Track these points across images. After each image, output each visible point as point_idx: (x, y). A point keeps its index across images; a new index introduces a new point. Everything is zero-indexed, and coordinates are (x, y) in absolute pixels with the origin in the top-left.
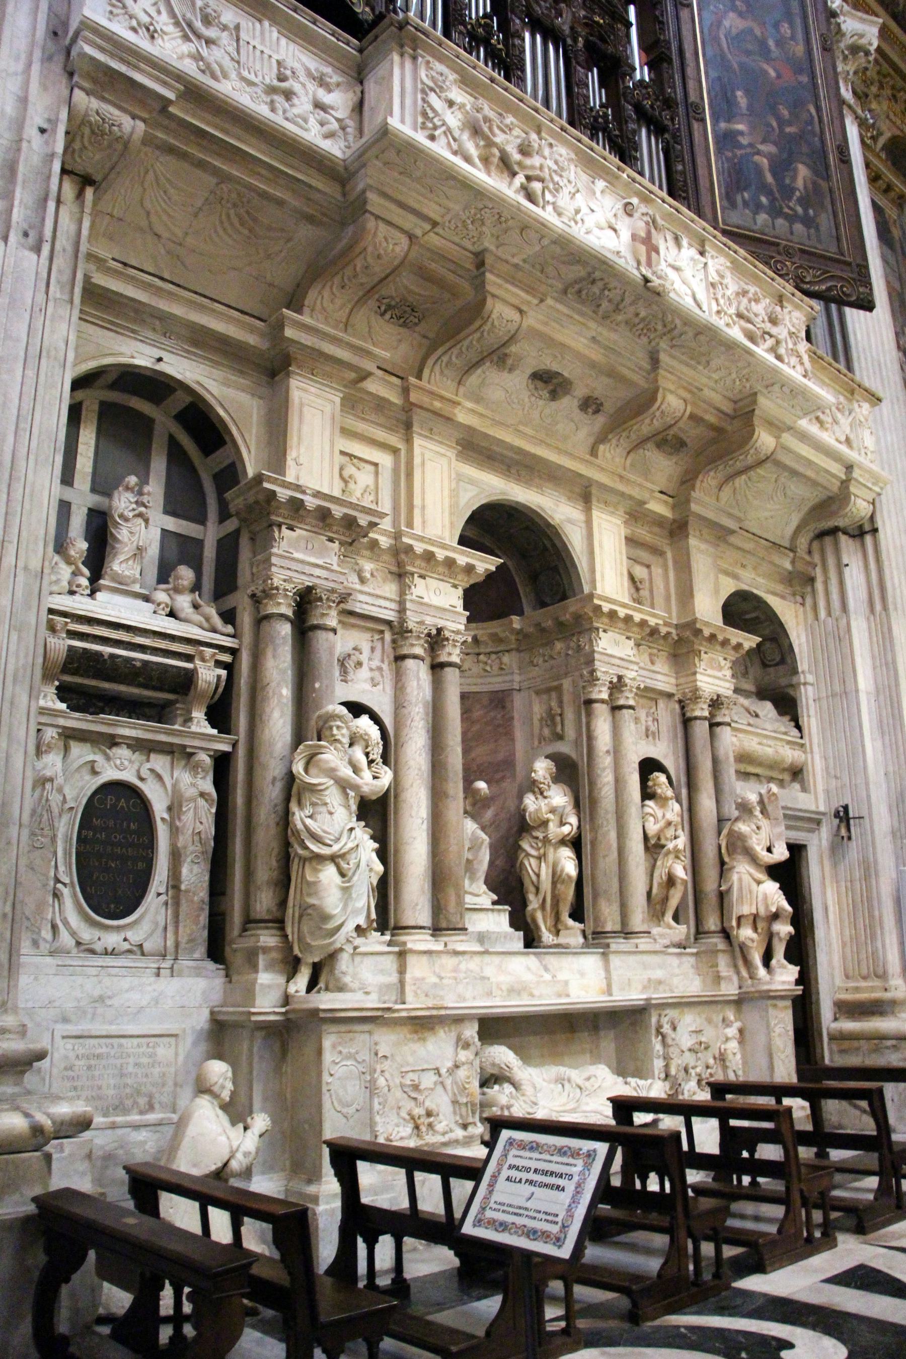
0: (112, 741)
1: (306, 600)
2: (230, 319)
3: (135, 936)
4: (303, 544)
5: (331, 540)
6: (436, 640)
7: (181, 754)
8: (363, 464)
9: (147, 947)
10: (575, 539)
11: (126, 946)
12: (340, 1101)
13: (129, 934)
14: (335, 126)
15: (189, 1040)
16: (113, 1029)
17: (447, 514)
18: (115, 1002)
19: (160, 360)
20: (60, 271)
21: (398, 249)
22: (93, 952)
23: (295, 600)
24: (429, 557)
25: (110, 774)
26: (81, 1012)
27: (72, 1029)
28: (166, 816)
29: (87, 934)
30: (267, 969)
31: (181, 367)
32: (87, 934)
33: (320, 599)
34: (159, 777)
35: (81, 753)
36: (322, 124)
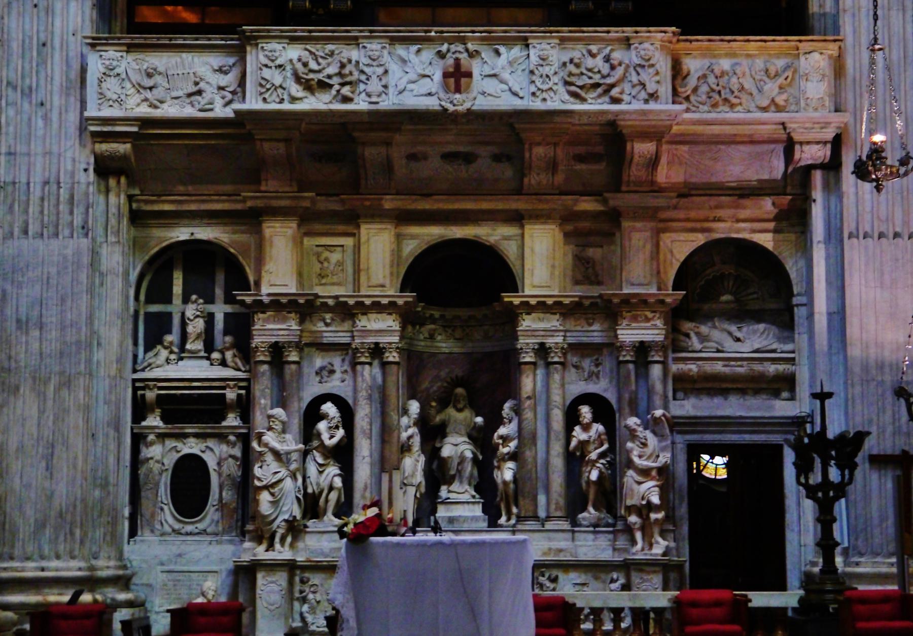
0: (186, 436)
1: (277, 350)
2: (224, 201)
3: (201, 526)
4: (272, 319)
5: (290, 312)
6: (377, 351)
7: (221, 437)
8: (333, 249)
9: (209, 530)
10: (510, 250)
11: (197, 531)
12: (268, 603)
13: (198, 525)
14: (229, 96)
15: (224, 574)
16: (185, 568)
17: (388, 266)
18: (187, 557)
19: (192, 234)
20: (112, 227)
21: (281, 151)
22: (181, 534)
23: (270, 352)
24: (360, 304)
25: (186, 450)
26: (170, 561)
27: (166, 568)
28: (216, 468)
29: (177, 526)
30: (250, 540)
31: (204, 233)
32: (177, 526)
33: (284, 347)
34: (212, 450)
35: (170, 443)
36: (223, 98)
